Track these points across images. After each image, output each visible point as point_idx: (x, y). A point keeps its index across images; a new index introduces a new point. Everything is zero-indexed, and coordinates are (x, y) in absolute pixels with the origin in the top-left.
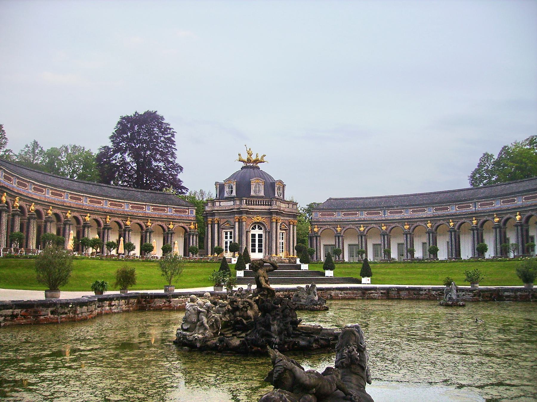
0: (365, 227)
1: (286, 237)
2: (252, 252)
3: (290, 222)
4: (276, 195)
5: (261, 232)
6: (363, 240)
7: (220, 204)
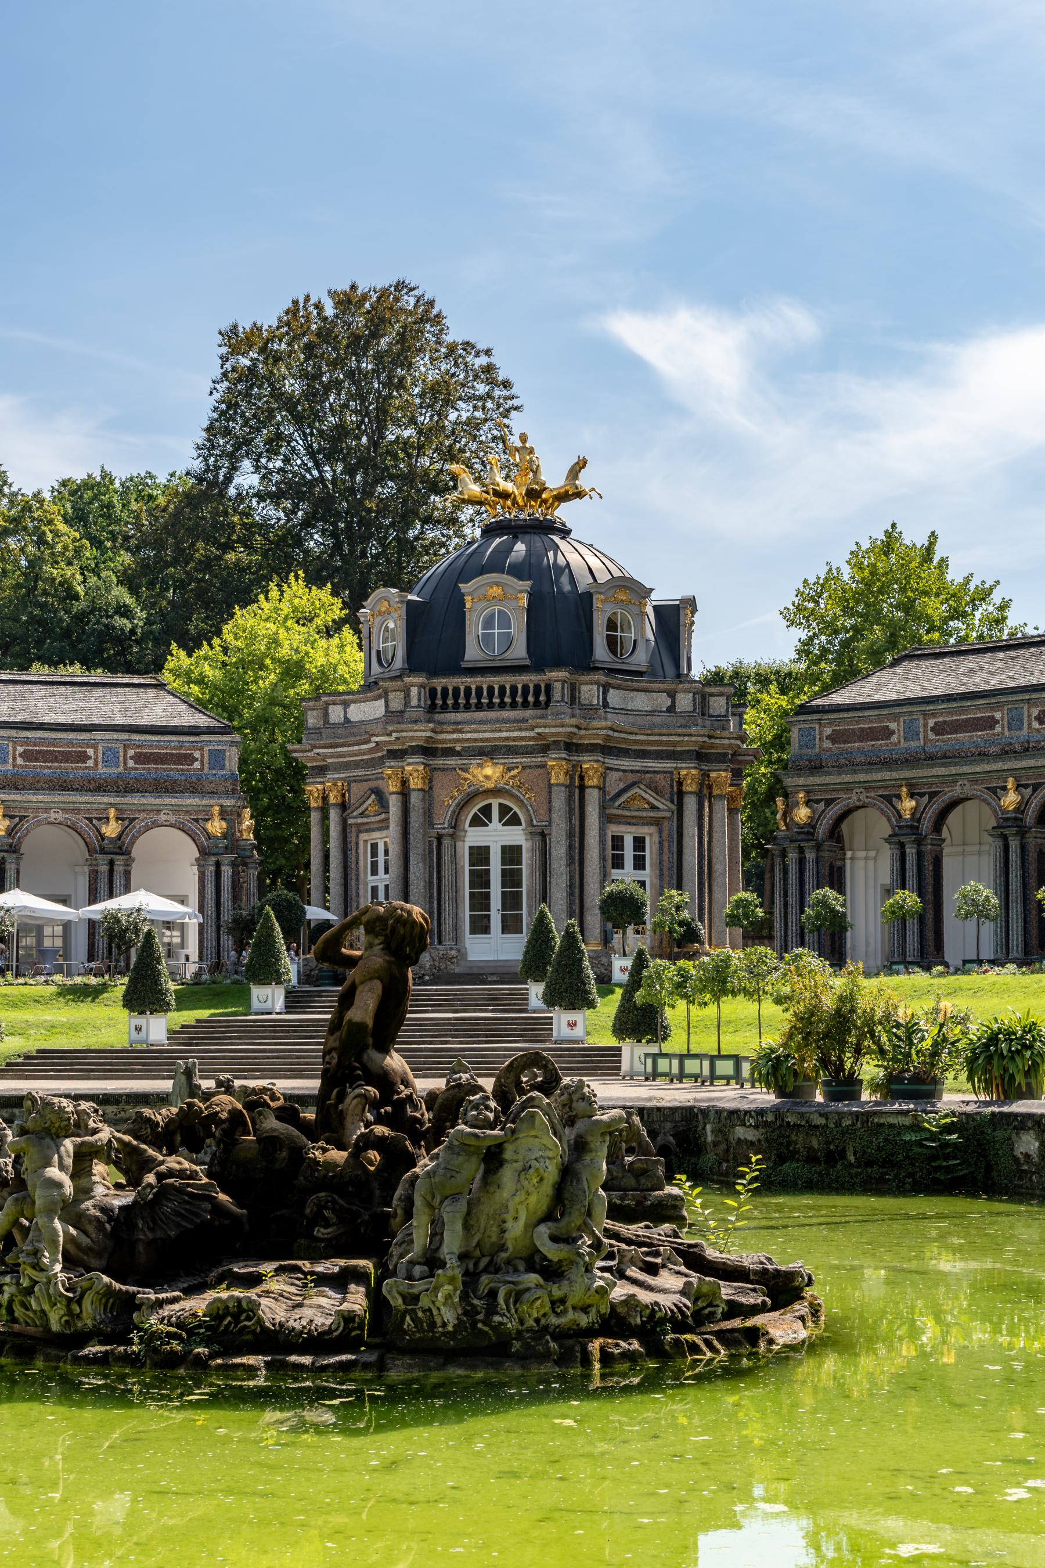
0: (1026, 786)
1: (661, 854)
2: (473, 931)
3: (680, 784)
4: (601, 652)
5: (516, 836)
6: (1014, 857)
7: (346, 713)
